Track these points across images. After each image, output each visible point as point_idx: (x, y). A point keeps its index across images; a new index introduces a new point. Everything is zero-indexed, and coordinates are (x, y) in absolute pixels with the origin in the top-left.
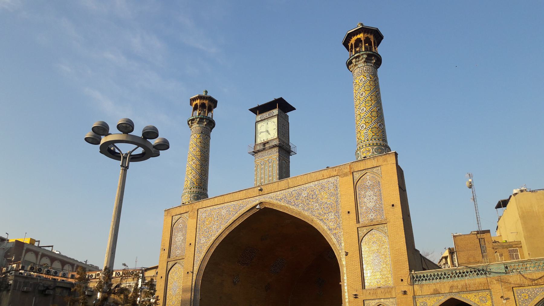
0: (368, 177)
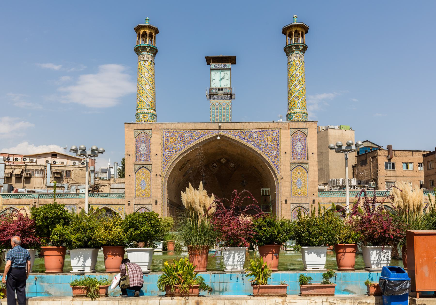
0: (299, 133)
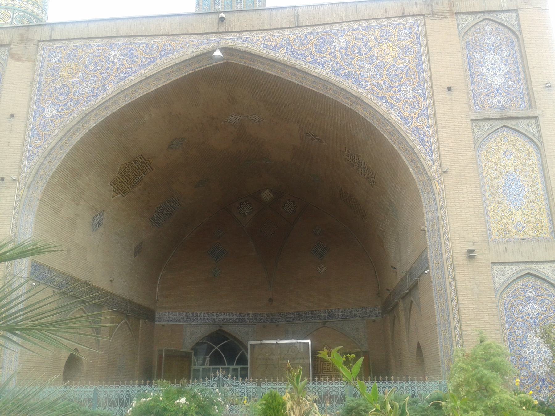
0: (488, 28)
